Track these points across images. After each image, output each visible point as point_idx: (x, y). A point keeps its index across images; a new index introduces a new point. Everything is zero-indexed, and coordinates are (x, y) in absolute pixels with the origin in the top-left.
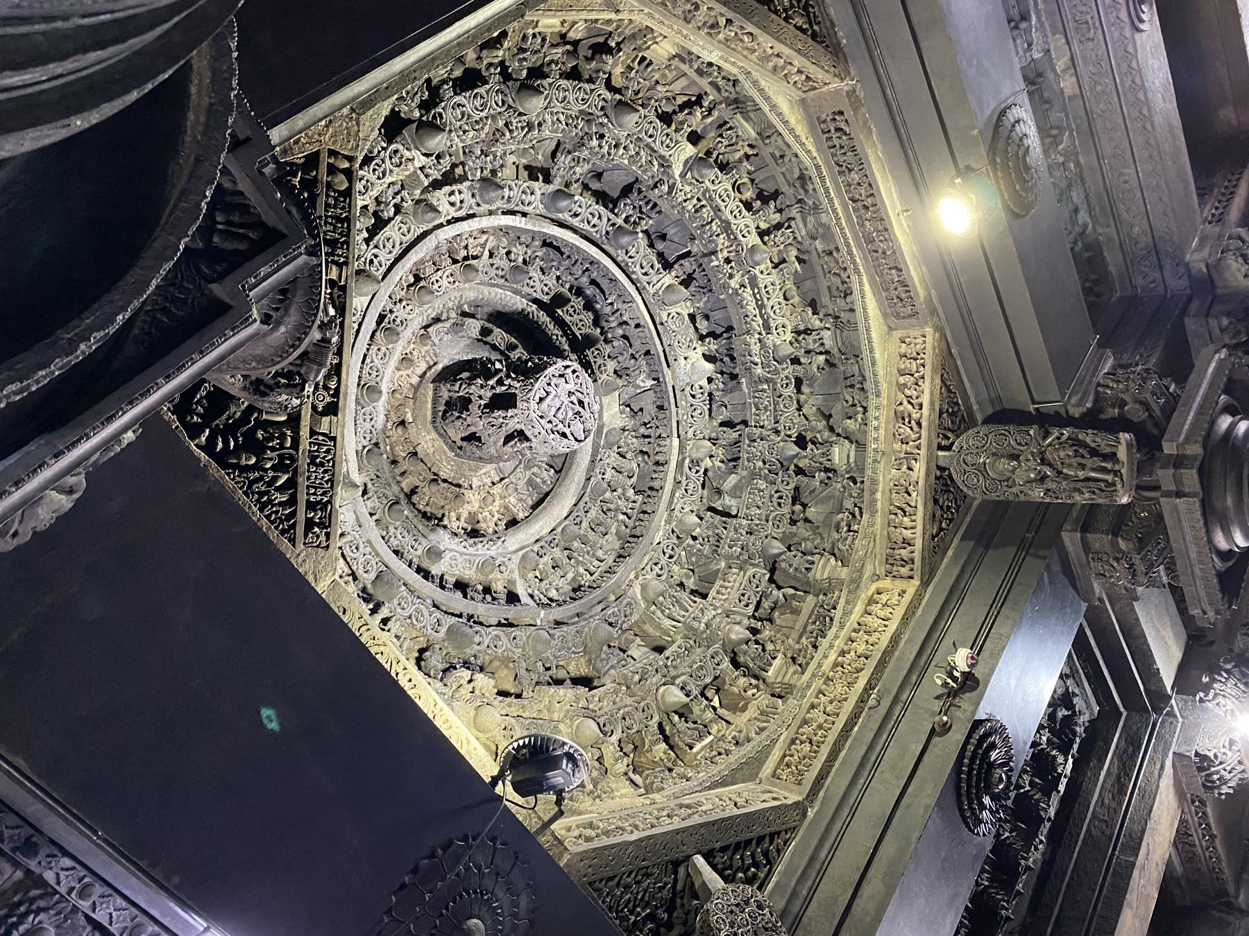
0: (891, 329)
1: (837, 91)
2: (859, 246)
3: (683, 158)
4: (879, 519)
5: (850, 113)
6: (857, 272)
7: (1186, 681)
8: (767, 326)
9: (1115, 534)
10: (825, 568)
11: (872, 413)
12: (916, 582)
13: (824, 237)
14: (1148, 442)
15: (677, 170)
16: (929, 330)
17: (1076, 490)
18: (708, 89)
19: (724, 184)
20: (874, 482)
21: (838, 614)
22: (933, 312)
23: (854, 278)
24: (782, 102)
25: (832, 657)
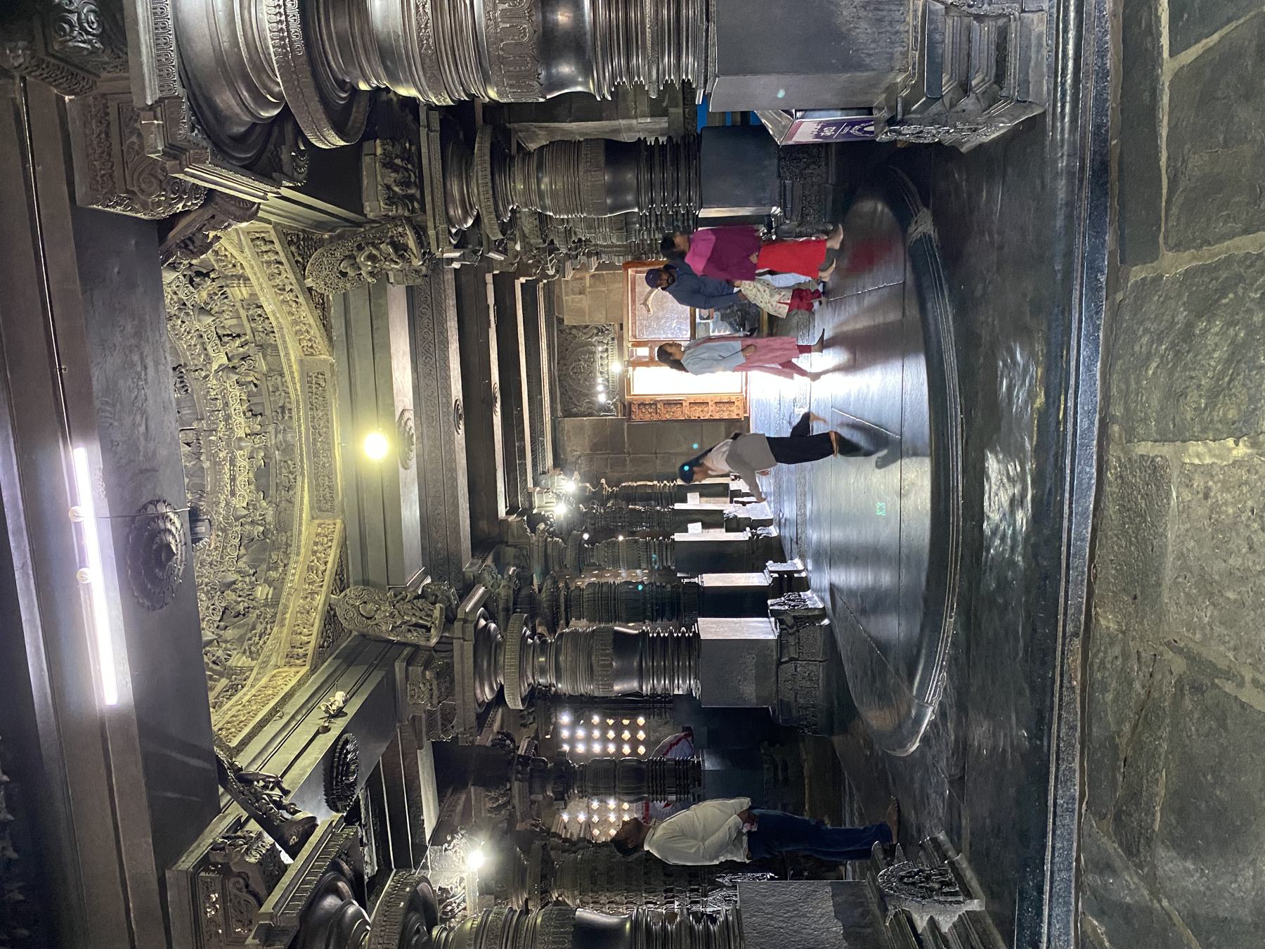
0: (313, 518)
1: (325, 361)
2: (308, 458)
3: (220, 362)
4: (285, 630)
5: (328, 375)
6: (303, 475)
7: (437, 838)
8: (233, 494)
9: (425, 669)
10: (239, 660)
11: (292, 565)
12: (307, 668)
13: (284, 450)
14: (450, 618)
15: (215, 366)
16: (339, 521)
17: (409, 631)
18: (249, 331)
19: (236, 391)
20: (286, 607)
21: (249, 682)
22: (343, 511)
23: (299, 479)
24: (292, 353)
25: (247, 698)
